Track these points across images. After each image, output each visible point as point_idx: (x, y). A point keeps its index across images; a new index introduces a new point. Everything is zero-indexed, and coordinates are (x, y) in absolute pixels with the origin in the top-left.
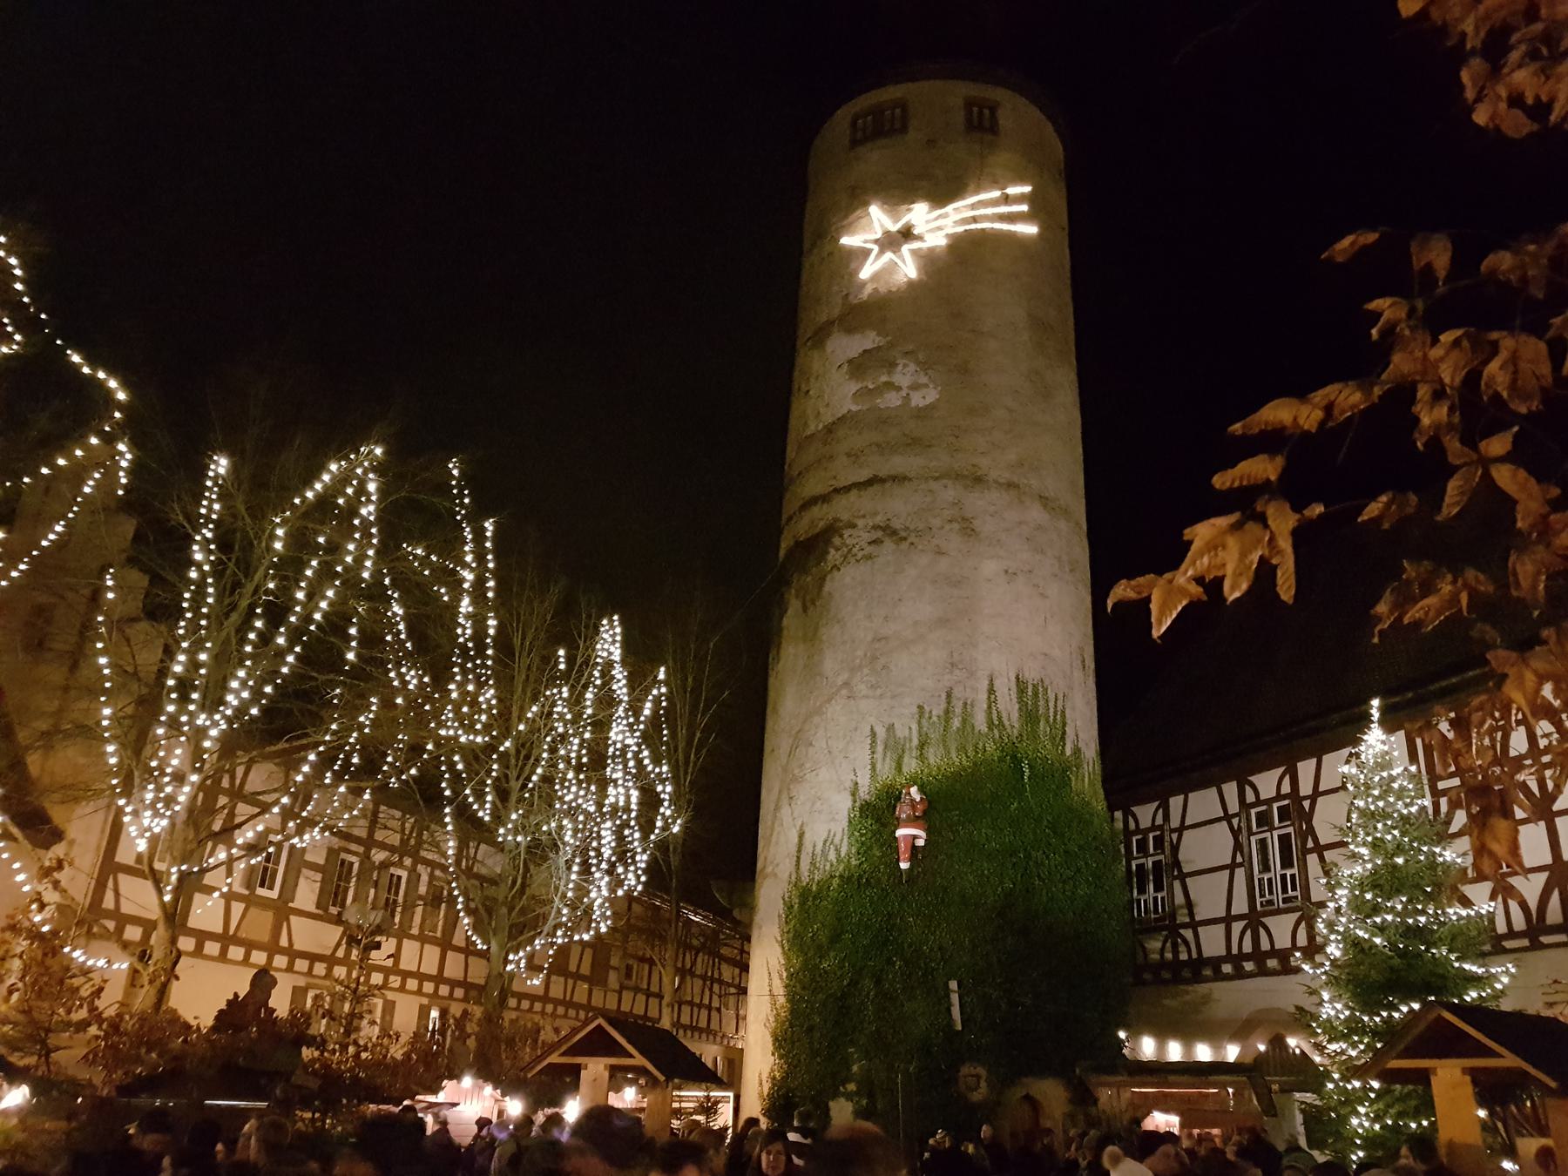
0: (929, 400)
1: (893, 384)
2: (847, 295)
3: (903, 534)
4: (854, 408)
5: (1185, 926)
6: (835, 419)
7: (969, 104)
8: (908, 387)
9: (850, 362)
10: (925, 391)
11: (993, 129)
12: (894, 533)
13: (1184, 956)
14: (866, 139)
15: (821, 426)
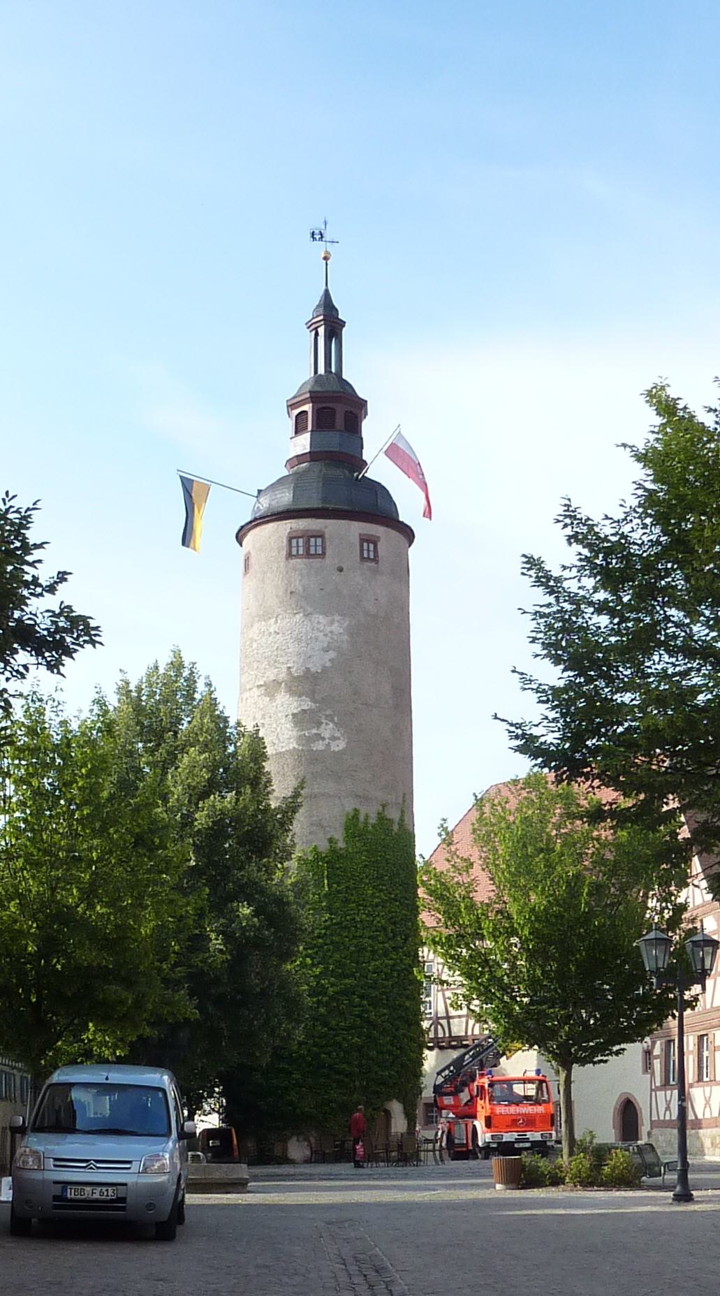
0: (341, 748)
1: (320, 735)
2: (289, 668)
3: (328, 829)
4: (297, 747)
5: (442, 1018)
6: (284, 750)
7: (366, 539)
8: (329, 738)
9: (293, 714)
10: (337, 742)
11: (375, 560)
12: (323, 827)
13: (440, 1035)
14: (297, 556)
15: (274, 752)
